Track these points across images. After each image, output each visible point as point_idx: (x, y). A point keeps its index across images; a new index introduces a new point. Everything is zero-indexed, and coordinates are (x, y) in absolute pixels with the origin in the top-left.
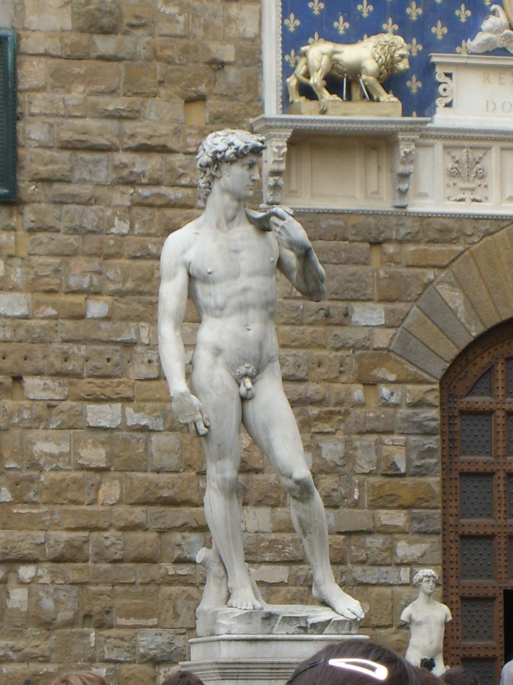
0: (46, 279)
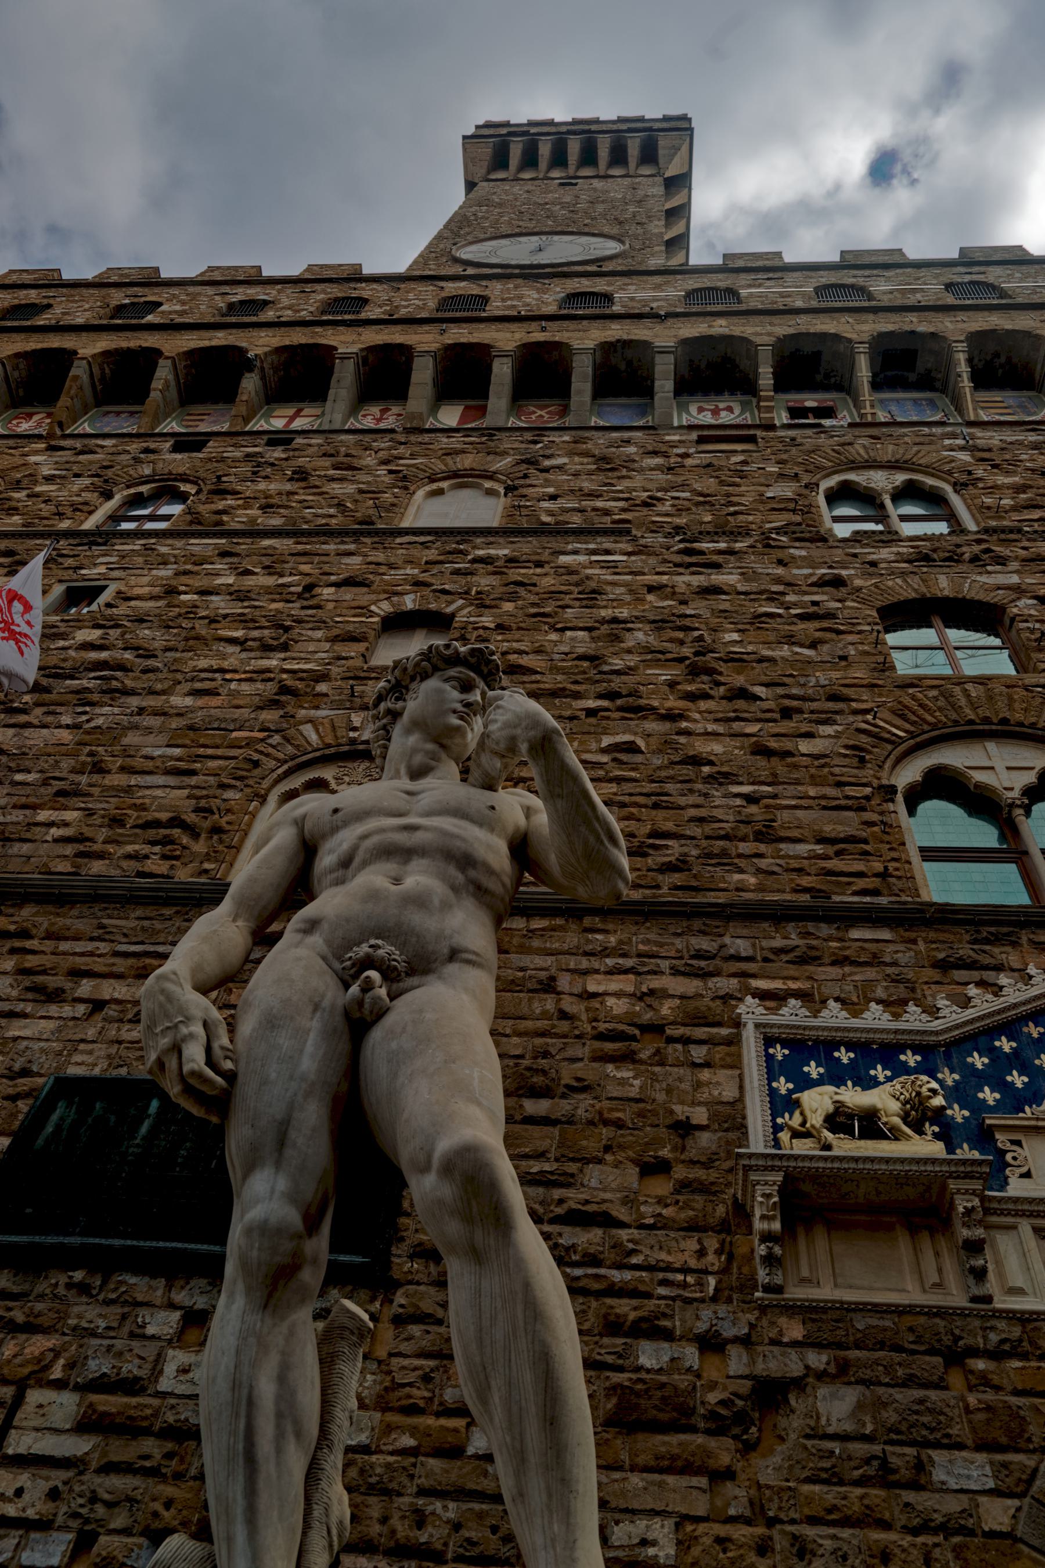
0: (407, 1389)
